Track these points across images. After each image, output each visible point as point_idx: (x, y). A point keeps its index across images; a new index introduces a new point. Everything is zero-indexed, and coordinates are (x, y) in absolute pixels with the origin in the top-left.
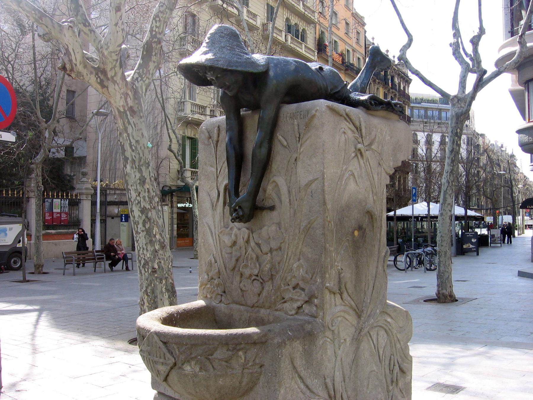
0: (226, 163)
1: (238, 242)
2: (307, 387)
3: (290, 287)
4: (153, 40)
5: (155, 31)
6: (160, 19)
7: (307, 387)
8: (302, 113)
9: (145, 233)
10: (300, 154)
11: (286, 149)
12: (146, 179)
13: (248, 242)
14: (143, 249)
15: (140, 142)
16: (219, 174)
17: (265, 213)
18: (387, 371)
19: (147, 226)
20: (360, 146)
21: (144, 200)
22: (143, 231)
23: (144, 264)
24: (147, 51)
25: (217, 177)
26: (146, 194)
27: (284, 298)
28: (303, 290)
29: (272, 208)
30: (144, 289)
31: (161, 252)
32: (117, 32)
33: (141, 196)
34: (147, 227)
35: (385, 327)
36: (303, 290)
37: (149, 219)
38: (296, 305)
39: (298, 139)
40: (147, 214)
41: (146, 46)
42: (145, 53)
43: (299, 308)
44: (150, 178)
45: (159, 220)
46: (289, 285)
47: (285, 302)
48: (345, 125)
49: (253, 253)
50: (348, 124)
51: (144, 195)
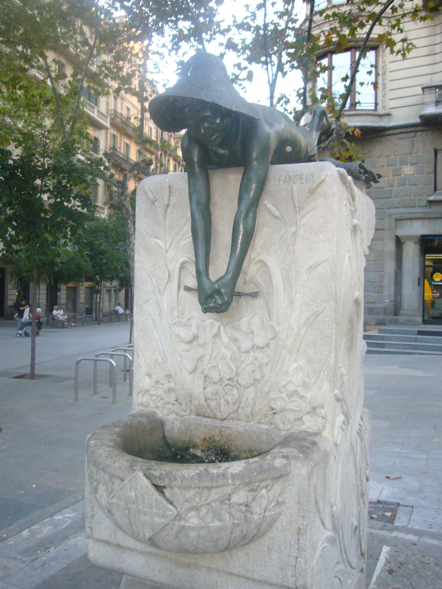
3: (284, 395)
8: (304, 176)
11: (278, 221)
13: (217, 336)
16: (169, 247)
17: (243, 299)
18: (359, 482)
20: (356, 221)
29: (255, 295)
48: (345, 194)
50: (348, 194)
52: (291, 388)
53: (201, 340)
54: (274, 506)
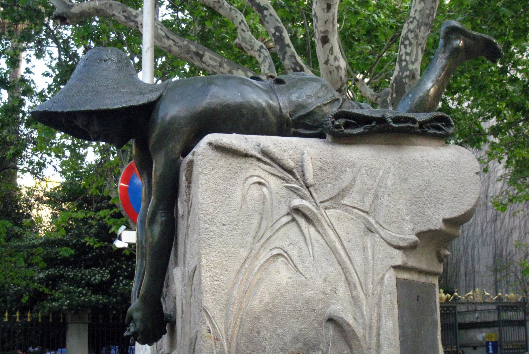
4: (403, 74)
5: (405, 60)
6: (410, 42)
32: (330, 72)
41: (394, 85)
42: (394, 95)
50: (267, 167)
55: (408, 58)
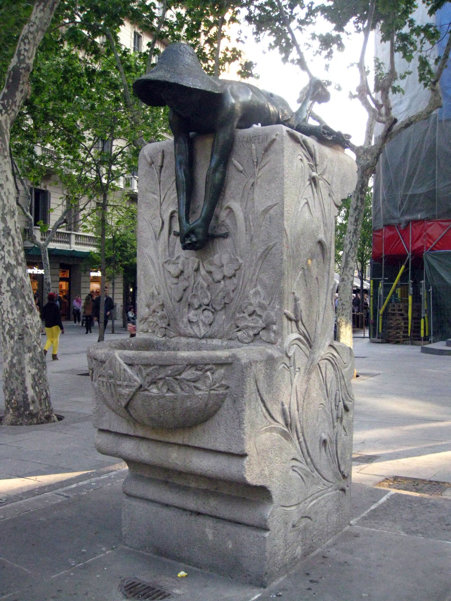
0: (175, 189)
1: (186, 272)
2: (268, 410)
3: (246, 315)
4: (20, 65)
5: (24, 55)
7: (268, 410)
8: (261, 137)
9: (10, 294)
10: (258, 179)
11: (242, 175)
12: (11, 230)
13: (197, 270)
14: (8, 312)
15: (5, 187)
17: (216, 240)
18: (333, 406)
19: (13, 285)
20: (314, 174)
21: (9, 255)
22: (7, 291)
23: (9, 330)
24: (13, 79)
25: (161, 205)
26: (11, 248)
27: (238, 327)
28: (260, 316)
29: (225, 236)
30: (9, 359)
31: (28, 316)
33: (5, 250)
34: (12, 287)
35: (332, 361)
36: (260, 316)
37: (15, 278)
38: (251, 333)
39: (255, 164)
40: (13, 271)
41: (12, 72)
42: (10, 81)
43: (255, 335)
44: (16, 230)
45: (26, 278)
46: (244, 312)
47: (239, 330)
48: (301, 152)
49: (204, 283)
50: (304, 151)
51: (9, 248)
52: (251, 309)
53: (185, 275)
54: (218, 387)
55: (26, 54)
